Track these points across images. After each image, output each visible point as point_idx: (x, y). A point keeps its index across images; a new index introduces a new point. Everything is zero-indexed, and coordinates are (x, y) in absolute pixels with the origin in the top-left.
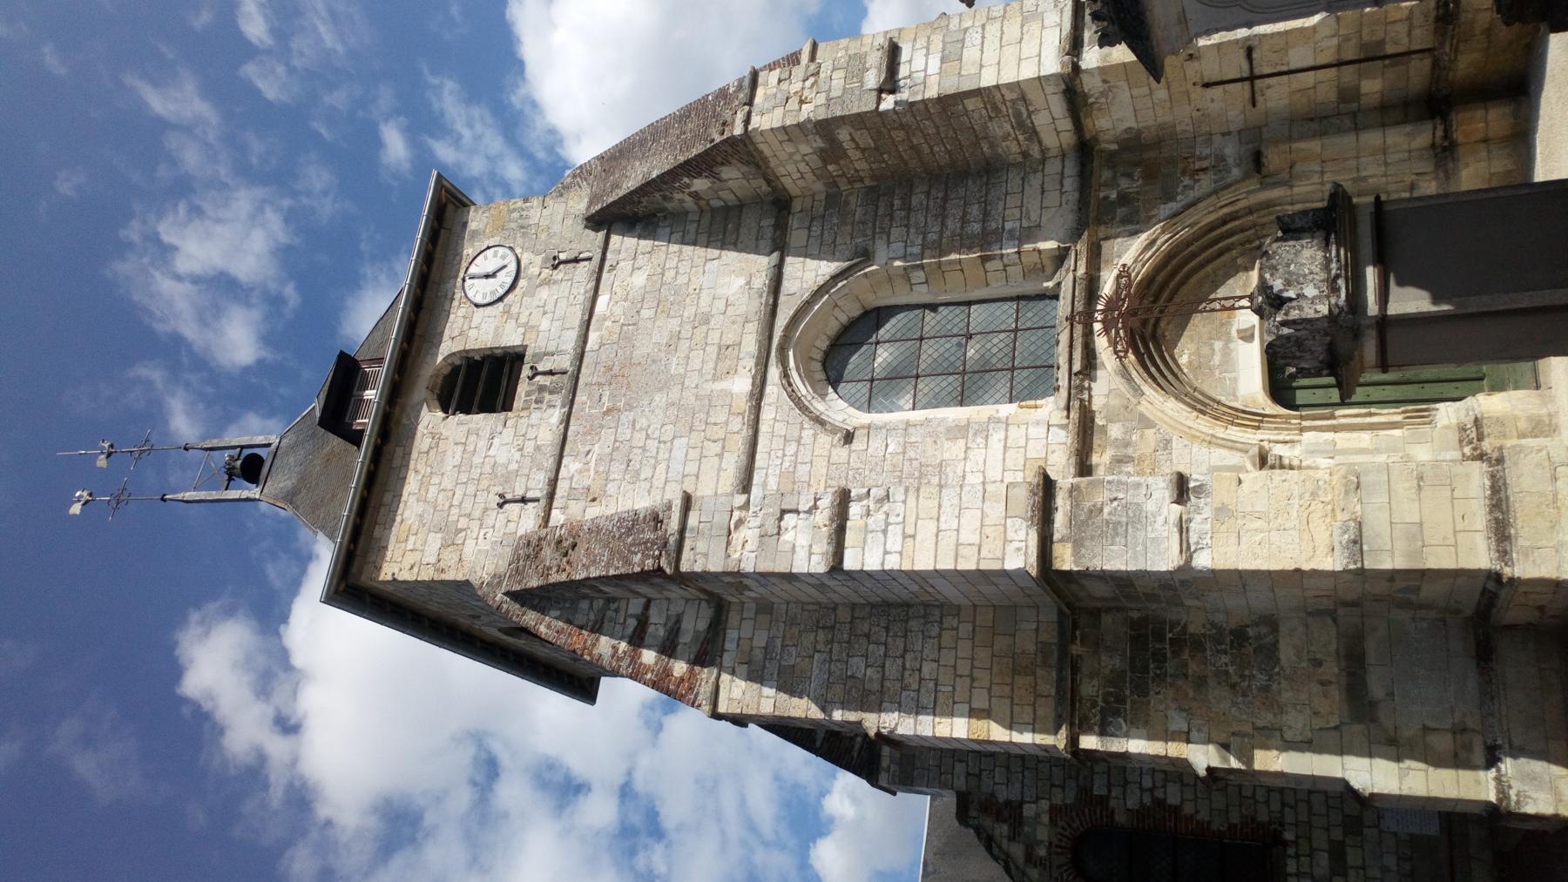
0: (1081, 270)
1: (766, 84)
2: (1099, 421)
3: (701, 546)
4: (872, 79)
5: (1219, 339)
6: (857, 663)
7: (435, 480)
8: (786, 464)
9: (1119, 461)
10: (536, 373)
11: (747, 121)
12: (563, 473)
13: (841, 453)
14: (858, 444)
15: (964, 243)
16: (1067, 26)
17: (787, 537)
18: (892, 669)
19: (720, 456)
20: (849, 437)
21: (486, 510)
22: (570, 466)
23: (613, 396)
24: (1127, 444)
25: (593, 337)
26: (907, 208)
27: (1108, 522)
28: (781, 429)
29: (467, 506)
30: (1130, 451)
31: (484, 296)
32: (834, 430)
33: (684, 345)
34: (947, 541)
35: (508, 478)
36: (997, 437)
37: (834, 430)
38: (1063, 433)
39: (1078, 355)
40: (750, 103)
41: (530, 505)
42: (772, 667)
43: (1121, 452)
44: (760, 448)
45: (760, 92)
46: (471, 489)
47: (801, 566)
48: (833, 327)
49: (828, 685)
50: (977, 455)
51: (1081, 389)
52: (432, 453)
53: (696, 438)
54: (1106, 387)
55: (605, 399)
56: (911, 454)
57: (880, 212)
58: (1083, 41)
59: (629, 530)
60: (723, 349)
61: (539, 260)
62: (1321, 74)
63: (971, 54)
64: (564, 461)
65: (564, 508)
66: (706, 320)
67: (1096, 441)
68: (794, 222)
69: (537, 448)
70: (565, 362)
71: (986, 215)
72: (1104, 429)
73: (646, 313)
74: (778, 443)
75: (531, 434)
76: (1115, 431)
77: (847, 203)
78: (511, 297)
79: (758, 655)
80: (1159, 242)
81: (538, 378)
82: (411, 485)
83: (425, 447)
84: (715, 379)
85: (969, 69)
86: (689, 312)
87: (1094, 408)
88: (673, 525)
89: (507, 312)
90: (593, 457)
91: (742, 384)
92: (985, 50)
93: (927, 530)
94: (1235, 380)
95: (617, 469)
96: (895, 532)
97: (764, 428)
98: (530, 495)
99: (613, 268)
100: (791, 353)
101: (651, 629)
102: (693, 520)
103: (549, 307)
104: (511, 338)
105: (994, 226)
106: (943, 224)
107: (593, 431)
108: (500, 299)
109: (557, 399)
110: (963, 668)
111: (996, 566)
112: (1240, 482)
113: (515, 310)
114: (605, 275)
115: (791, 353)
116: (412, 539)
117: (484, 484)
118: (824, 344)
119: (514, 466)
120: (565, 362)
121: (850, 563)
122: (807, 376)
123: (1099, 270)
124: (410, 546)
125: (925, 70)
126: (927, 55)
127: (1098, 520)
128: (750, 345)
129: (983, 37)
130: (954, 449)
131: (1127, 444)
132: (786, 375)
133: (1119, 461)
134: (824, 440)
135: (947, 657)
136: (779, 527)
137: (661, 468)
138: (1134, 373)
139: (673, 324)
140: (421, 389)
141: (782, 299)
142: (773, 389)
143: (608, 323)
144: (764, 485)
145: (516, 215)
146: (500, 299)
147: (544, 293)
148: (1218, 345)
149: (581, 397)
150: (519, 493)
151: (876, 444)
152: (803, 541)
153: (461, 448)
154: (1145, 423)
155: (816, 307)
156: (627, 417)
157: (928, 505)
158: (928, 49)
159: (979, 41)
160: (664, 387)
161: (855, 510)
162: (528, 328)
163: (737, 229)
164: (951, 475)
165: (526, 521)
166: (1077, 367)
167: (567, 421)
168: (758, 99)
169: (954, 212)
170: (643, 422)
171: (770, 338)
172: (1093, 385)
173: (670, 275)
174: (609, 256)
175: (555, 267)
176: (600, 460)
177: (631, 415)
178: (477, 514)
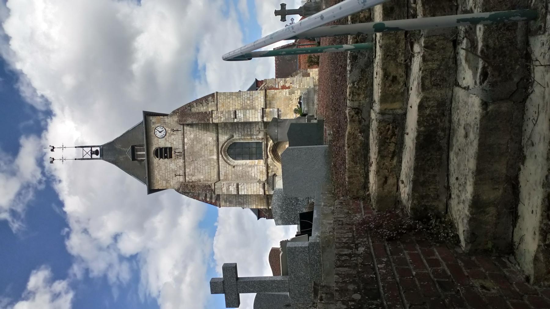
0: (265, 143)
1: (214, 114)
3: (218, 191)
4: (232, 116)
6: (240, 200)
7: (161, 171)
10: (175, 152)
11: (212, 121)
12: (186, 171)
13: (233, 169)
14: (236, 168)
15: (248, 135)
16: (262, 114)
17: (230, 189)
18: (245, 200)
19: (214, 169)
20: (234, 167)
21: (173, 177)
22: (187, 170)
23: (192, 158)
25: (186, 147)
26: (238, 128)
28: (223, 165)
29: (169, 176)
31: (160, 136)
32: (232, 166)
33: (203, 150)
34: (252, 190)
35: (175, 171)
36: (256, 168)
37: (232, 166)
39: (266, 156)
40: (212, 117)
41: (181, 176)
42: (228, 201)
44: (220, 168)
45: (213, 115)
46: (169, 173)
47: (233, 193)
48: (228, 146)
49: (236, 203)
50: (253, 170)
51: (267, 161)
52: (159, 167)
53: (209, 166)
54: (270, 160)
55: (191, 158)
56: (244, 170)
57: (234, 128)
59: (205, 187)
61: (170, 129)
63: (248, 115)
64: (186, 169)
65: (188, 177)
66: (206, 145)
67: (269, 168)
68: (219, 128)
69: (180, 166)
70: (181, 150)
71: (251, 131)
73: (195, 143)
74: (223, 167)
75: (178, 164)
76: (271, 167)
77: (228, 126)
78: (165, 137)
79: (225, 199)
81: (176, 153)
82: (156, 172)
83: (157, 166)
84: (210, 156)
85: (248, 118)
86: (203, 143)
88: (213, 188)
89: (166, 139)
90: (191, 169)
91: (215, 157)
93: (250, 189)
95: (196, 171)
96: (245, 190)
97: (220, 165)
98: (180, 174)
99: (186, 133)
101: (207, 196)
102: (216, 187)
103: (175, 139)
104: (169, 145)
105: (252, 133)
106: (244, 132)
107: (190, 164)
108: (164, 137)
109: (182, 158)
110: (254, 200)
111: (259, 194)
113: (167, 139)
114: (185, 135)
116: (160, 182)
117: (171, 172)
119: (176, 169)
120: (181, 150)
121: (240, 193)
122: (226, 156)
124: (160, 183)
128: (215, 150)
130: (250, 169)
132: (222, 156)
133: (272, 171)
134: (230, 167)
135: (252, 198)
137: (204, 171)
139: (200, 145)
140: (152, 155)
141: (219, 142)
142: (220, 158)
143: (188, 144)
144: (222, 174)
145: (162, 120)
146: (164, 137)
147: (173, 137)
149: (186, 158)
150: (178, 174)
151: (238, 168)
152: (233, 190)
153: (164, 166)
154: (275, 166)
156: (196, 162)
157: (249, 186)
160: (201, 157)
161: (240, 186)
162: (171, 143)
163: (209, 127)
165: (181, 179)
166: (266, 158)
167: (185, 162)
168: (213, 116)
169: (246, 130)
170: (199, 163)
173: (198, 136)
174: (185, 131)
175: (174, 131)
176: (193, 169)
177: (197, 162)
178: (171, 178)
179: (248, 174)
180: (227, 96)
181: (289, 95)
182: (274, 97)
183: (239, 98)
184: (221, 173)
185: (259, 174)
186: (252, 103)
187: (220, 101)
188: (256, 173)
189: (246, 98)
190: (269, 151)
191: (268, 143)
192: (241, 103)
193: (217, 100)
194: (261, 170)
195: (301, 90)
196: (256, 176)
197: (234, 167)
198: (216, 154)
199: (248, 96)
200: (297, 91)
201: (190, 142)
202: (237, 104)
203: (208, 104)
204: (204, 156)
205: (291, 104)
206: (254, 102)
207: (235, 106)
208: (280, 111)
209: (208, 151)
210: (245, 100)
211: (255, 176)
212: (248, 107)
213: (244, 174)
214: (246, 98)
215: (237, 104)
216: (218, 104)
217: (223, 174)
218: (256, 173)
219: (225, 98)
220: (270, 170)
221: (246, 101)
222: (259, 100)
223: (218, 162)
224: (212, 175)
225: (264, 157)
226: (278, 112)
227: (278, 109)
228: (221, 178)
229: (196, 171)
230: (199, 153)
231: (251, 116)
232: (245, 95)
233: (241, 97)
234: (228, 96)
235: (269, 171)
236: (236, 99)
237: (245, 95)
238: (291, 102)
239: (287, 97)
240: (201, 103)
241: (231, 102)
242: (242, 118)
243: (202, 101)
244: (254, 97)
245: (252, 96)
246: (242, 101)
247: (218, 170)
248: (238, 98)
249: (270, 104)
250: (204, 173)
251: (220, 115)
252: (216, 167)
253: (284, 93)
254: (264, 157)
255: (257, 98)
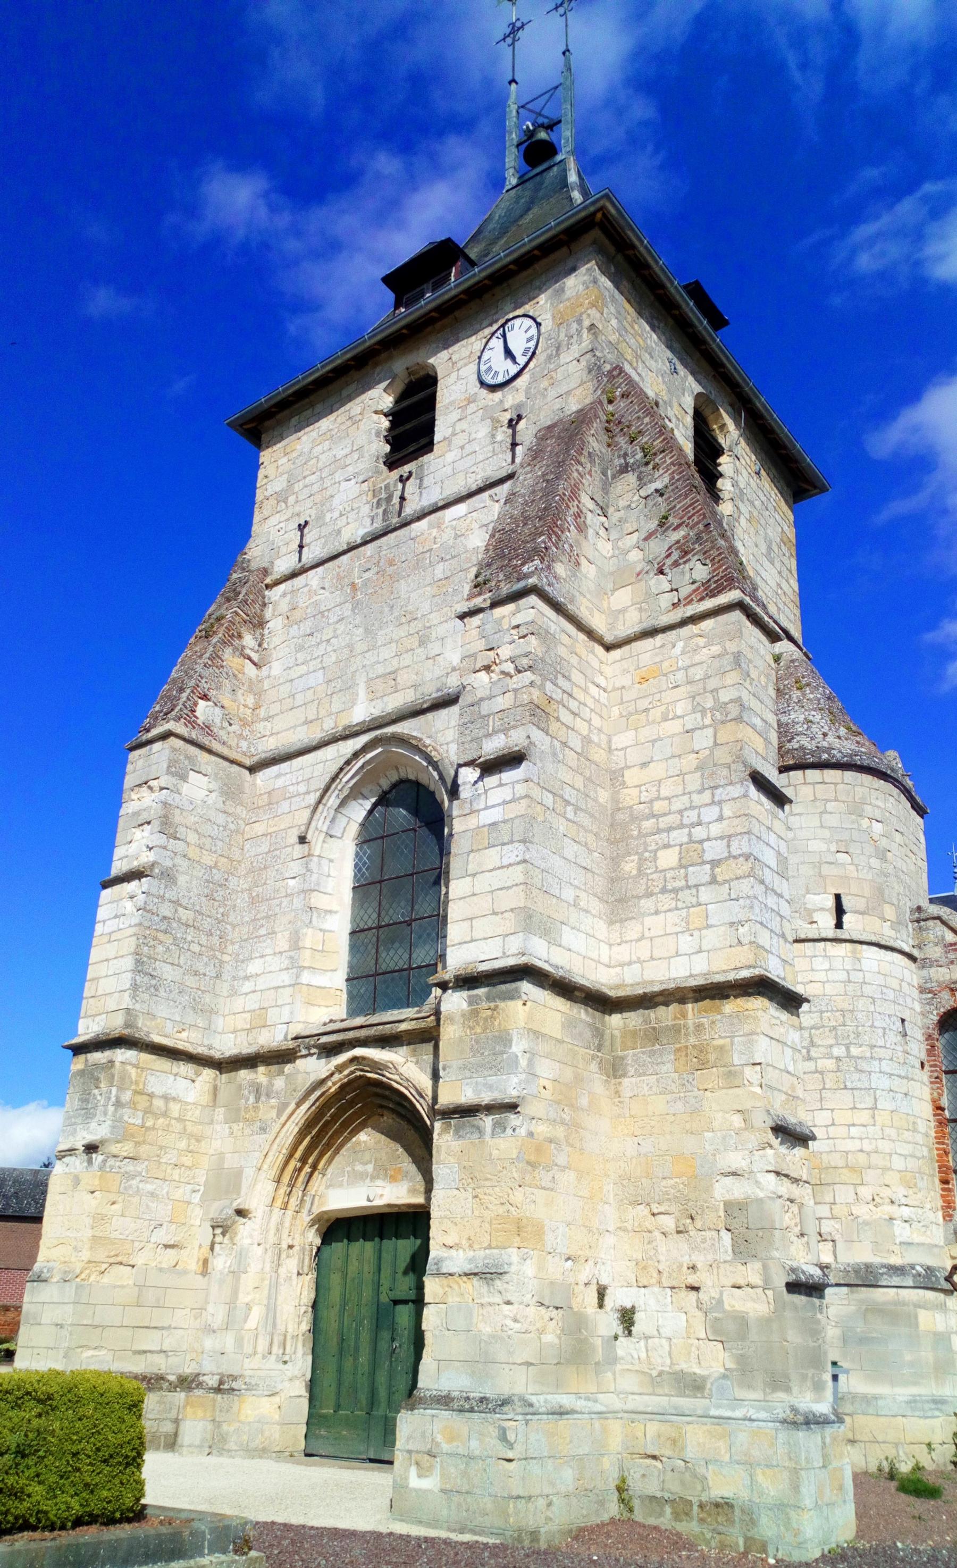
2: (288, 1068)
5: (374, 1169)
8: (291, 789)
9: (257, 1091)
14: (298, 847)
19: (307, 722)
24: (268, 1095)
27: (89, 1094)
30: (263, 1098)
36: (286, 978)
38: (281, 1037)
40: (494, 605)
43: (264, 1093)
56: (285, 902)
58: (476, 988)
60: (393, 675)
62: (884, 1284)
63: (492, 857)
67: (274, 1068)
72: (281, 1073)
76: (279, 1083)
80: (421, 1100)
87: (298, 1062)
91: (360, 713)
92: (494, 873)
94: (341, 1186)
100: (380, 750)
112: (92, 1192)
115: (380, 750)
118: (412, 777)
122: (368, 776)
123: (409, 1044)
125: (486, 808)
126: (505, 803)
127: (93, 1087)
129: (510, 865)
130: (282, 942)
131: (268, 1095)
132: (356, 755)
133: (257, 1091)
136: (142, 825)
138: (318, 1093)
141: (429, 716)
148: (370, 1168)
151: (295, 867)
155: (417, 758)
156: (347, 609)
158: (509, 802)
159: (505, 862)
161: (135, 883)
164: (265, 944)
170: (341, 628)
171: (394, 722)
172: (315, 1056)
179: (263, 931)
180: (712, 683)
181: (728, 1205)
182: (703, 1065)
183: (694, 782)
184: (285, 766)
185: (252, 1003)
186: (664, 890)
187: (680, 645)
188: (261, 983)
189: (699, 832)
190: (354, 1060)
191: (404, 1050)
192: (658, 806)
193: (684, 623)
194: (273, 1015)
195: (766, 1322)
196: (248, 986)
197: (302, 840)
198: (377, 712)
199: (714, 850)
200: (756, 1280)
201: (447, 536)
202: (657, 770)
203: (661, 572)
204: (372, 648)
205: (650, 1222)
206: (666, 901)
207: (644, 765)
208: (500, 1127)
209: (395, 662)
210: (681, 826)
211: (247, 978)
212: (630, 866)
213: (264, 907)
214: (699, 832)
215: (657, 770)
216: (659, 639)
217: (280, 783)
218: (261, 983)
219: (698, 673)
220: (269, 1075)
221: (674, 834)
222: (686, 943)
223: (335, 739)
224: (279, 724)
225: (359, 1021)
226: (490, 1109)
227: (512, 1107)
228: (262, 777)
229: (306, 627)
230: (387, 609)
231: (484, 883)
232: (720, 818)
233: (706, 797)
234: (715, 690)
235: (261, 1069)
236: (690, 761)
237: (720, 818)
238: (668, 1223)
239: (708, 1189)
240: (661, 525)
241: (674, 727)
242: (472, 822)
243: (676, 522)
244: (705, 895)
245: (713, 881)
246: (677, 805)
247: (298, 746)
248: (697, 769)
249: (653, 1036)
250: (294, 673)
251: (505, 652)
252: (315, 734)
253: (736, 1160)
254: (359, 1021)
255: (696, 922)
